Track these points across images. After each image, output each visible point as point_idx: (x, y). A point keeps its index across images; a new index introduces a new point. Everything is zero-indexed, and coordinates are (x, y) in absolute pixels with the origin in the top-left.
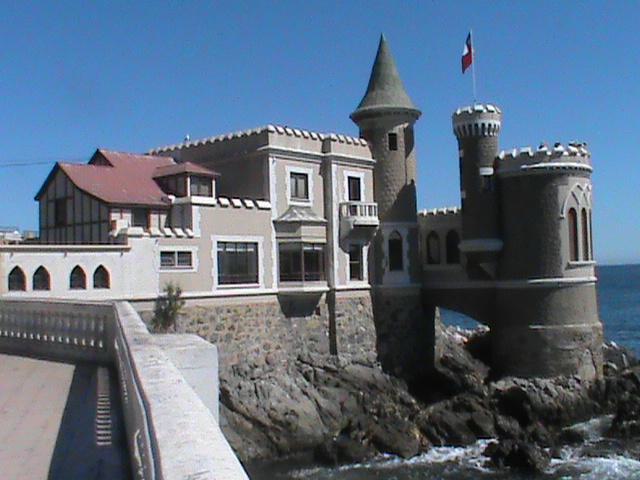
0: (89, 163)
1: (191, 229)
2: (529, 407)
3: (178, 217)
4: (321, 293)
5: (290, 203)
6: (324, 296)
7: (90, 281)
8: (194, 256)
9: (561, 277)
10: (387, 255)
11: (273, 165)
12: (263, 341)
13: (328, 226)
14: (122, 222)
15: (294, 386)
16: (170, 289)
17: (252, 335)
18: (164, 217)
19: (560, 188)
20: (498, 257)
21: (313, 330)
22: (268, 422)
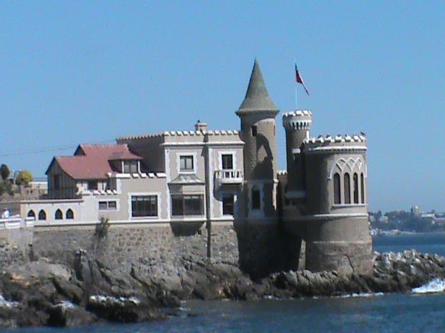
0: (75, 154)
1: (116, 190)
3: (111, 184)
4: (203, 222)
5: (179, 173)
6: (205, 224)
7: (64, 216)
8: (117, 203)
9: (328, 213)
11: (167, 153)
12: (159, 247)
13: (207, 184)
14: (82, 188)
16: (102, 219)
18: (105, 184)
19: (328, 162)
20: (303, 201)
22: (149, 283)
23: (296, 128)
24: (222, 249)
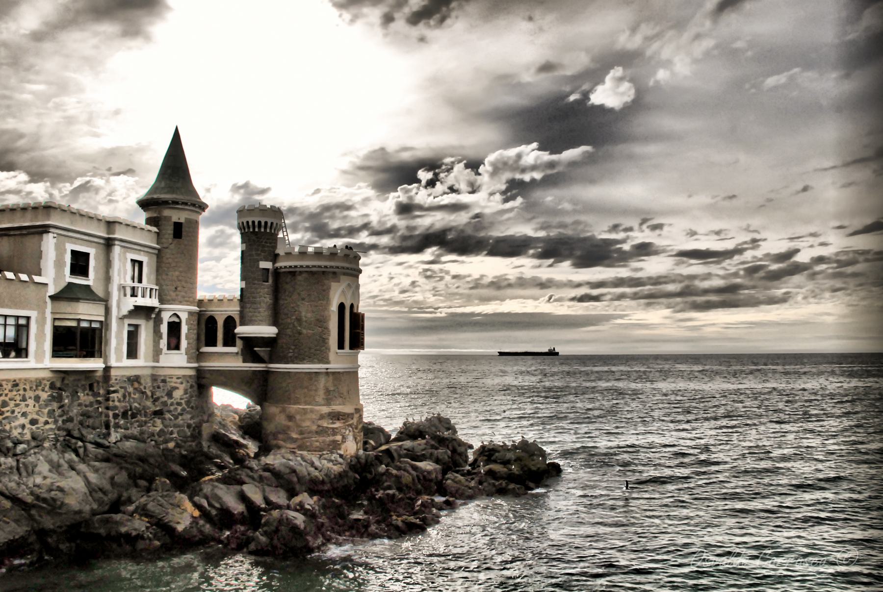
2: (295, 479)
5: (69, 279)
9: (328, 363)
12: (29, 417)
15: (62, 461)
17: (17, 410)
21: (86, 406)
22: (29, 499)
23: (263, 230)
24: (125, 415)
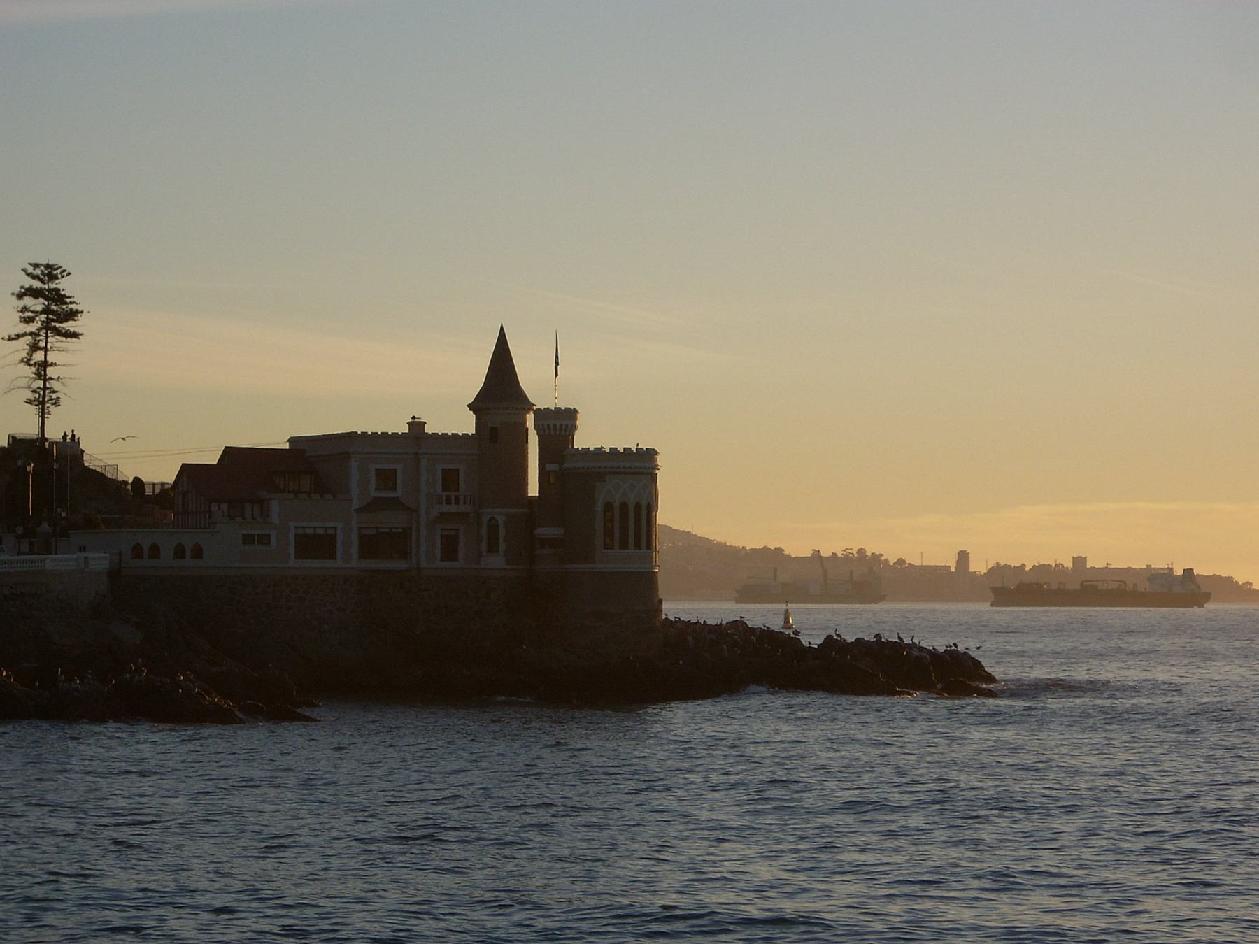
5: (374, 494)
7: (188, 553)
8: (273, 541)
10: (501, 539)
